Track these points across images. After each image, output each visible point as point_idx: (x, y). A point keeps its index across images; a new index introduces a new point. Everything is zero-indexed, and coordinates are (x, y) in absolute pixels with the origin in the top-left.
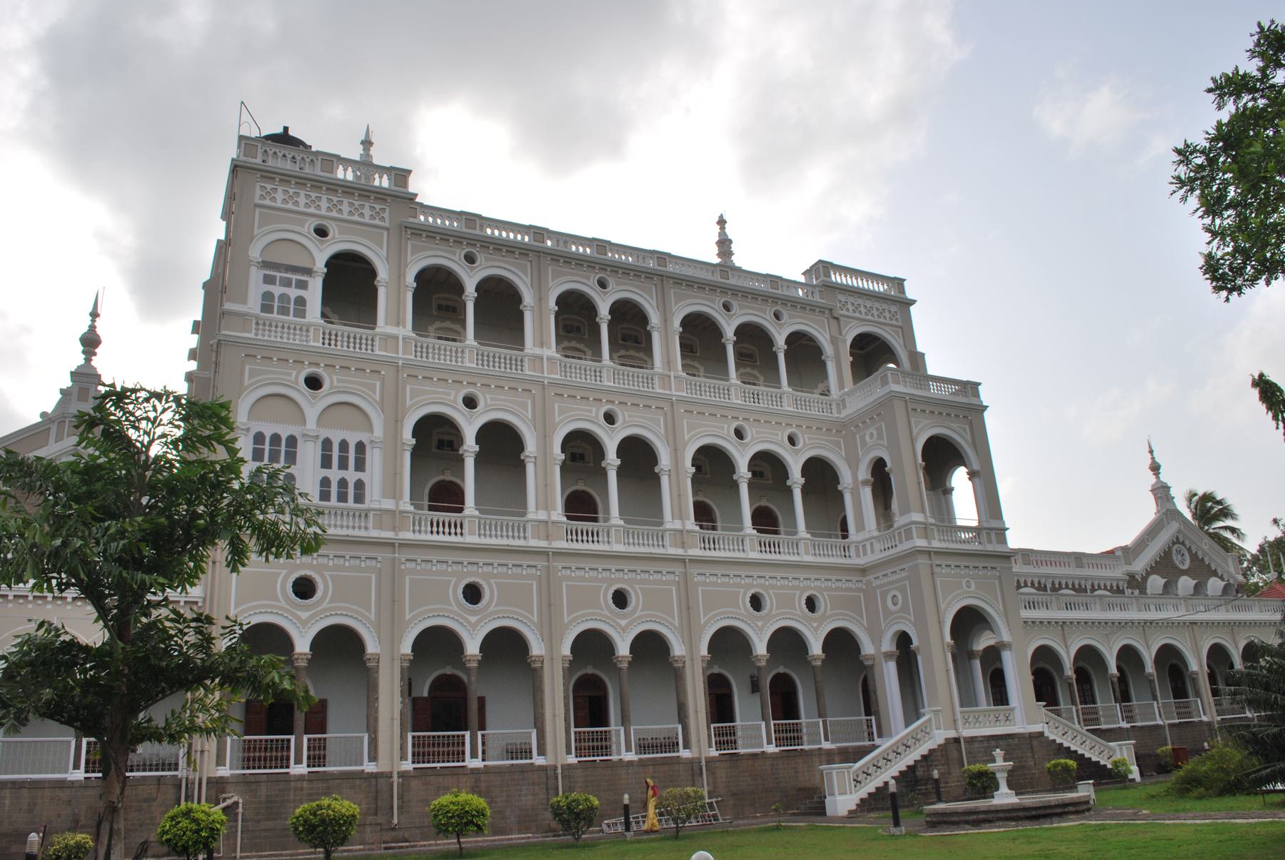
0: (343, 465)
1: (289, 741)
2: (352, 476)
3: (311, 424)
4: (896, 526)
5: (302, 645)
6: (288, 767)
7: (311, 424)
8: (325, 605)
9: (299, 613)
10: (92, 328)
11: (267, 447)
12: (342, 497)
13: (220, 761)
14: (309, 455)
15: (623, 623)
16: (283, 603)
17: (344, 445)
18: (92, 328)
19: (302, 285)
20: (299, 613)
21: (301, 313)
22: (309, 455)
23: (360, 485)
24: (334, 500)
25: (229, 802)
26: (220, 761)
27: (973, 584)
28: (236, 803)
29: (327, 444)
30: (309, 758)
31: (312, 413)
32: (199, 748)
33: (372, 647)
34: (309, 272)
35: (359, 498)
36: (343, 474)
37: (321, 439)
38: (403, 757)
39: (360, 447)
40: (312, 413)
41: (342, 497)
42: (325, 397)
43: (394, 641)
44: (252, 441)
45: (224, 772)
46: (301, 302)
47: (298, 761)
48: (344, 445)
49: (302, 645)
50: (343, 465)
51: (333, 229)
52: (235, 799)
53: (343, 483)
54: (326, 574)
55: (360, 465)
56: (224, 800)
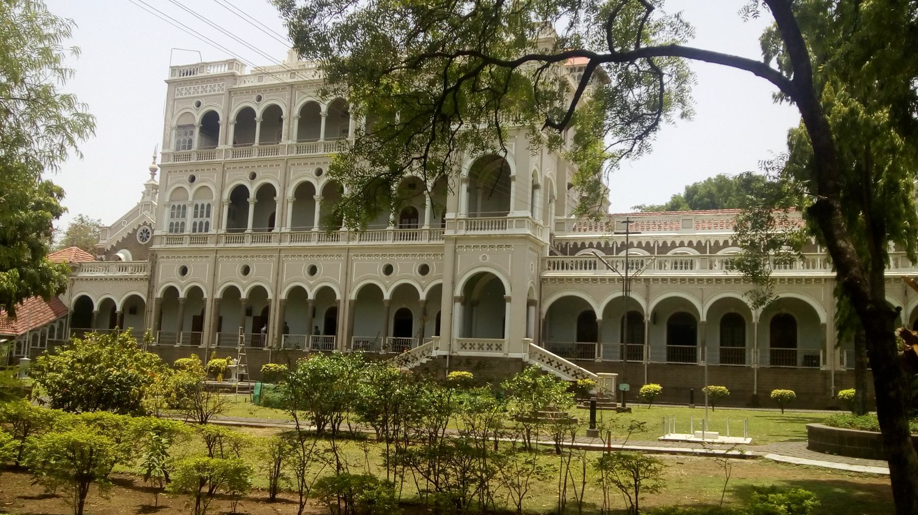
0: (202, 216)
3: (190, 199)
4: (509, 216)
7: (190, 199)
14: (190, 211)
15: (312, 282)
17: (203, 206)
19: (192, 133)
21: (190, 147)
22: (190, 211)
27: (488, 258)
29: (197, 207)
31: (191, 193)
33: (205, 296)
34: (193, 126)
35: (207, 230)
36: (201, 219)
38: (213, 342)
39: (209, 205)
40: (191, 193)
42: (197, 185)
43: (213, 292)
46: (190, 141)
48: (203, 206)
50: (202, 216)
51: (203, 104)
53: (201, 223)
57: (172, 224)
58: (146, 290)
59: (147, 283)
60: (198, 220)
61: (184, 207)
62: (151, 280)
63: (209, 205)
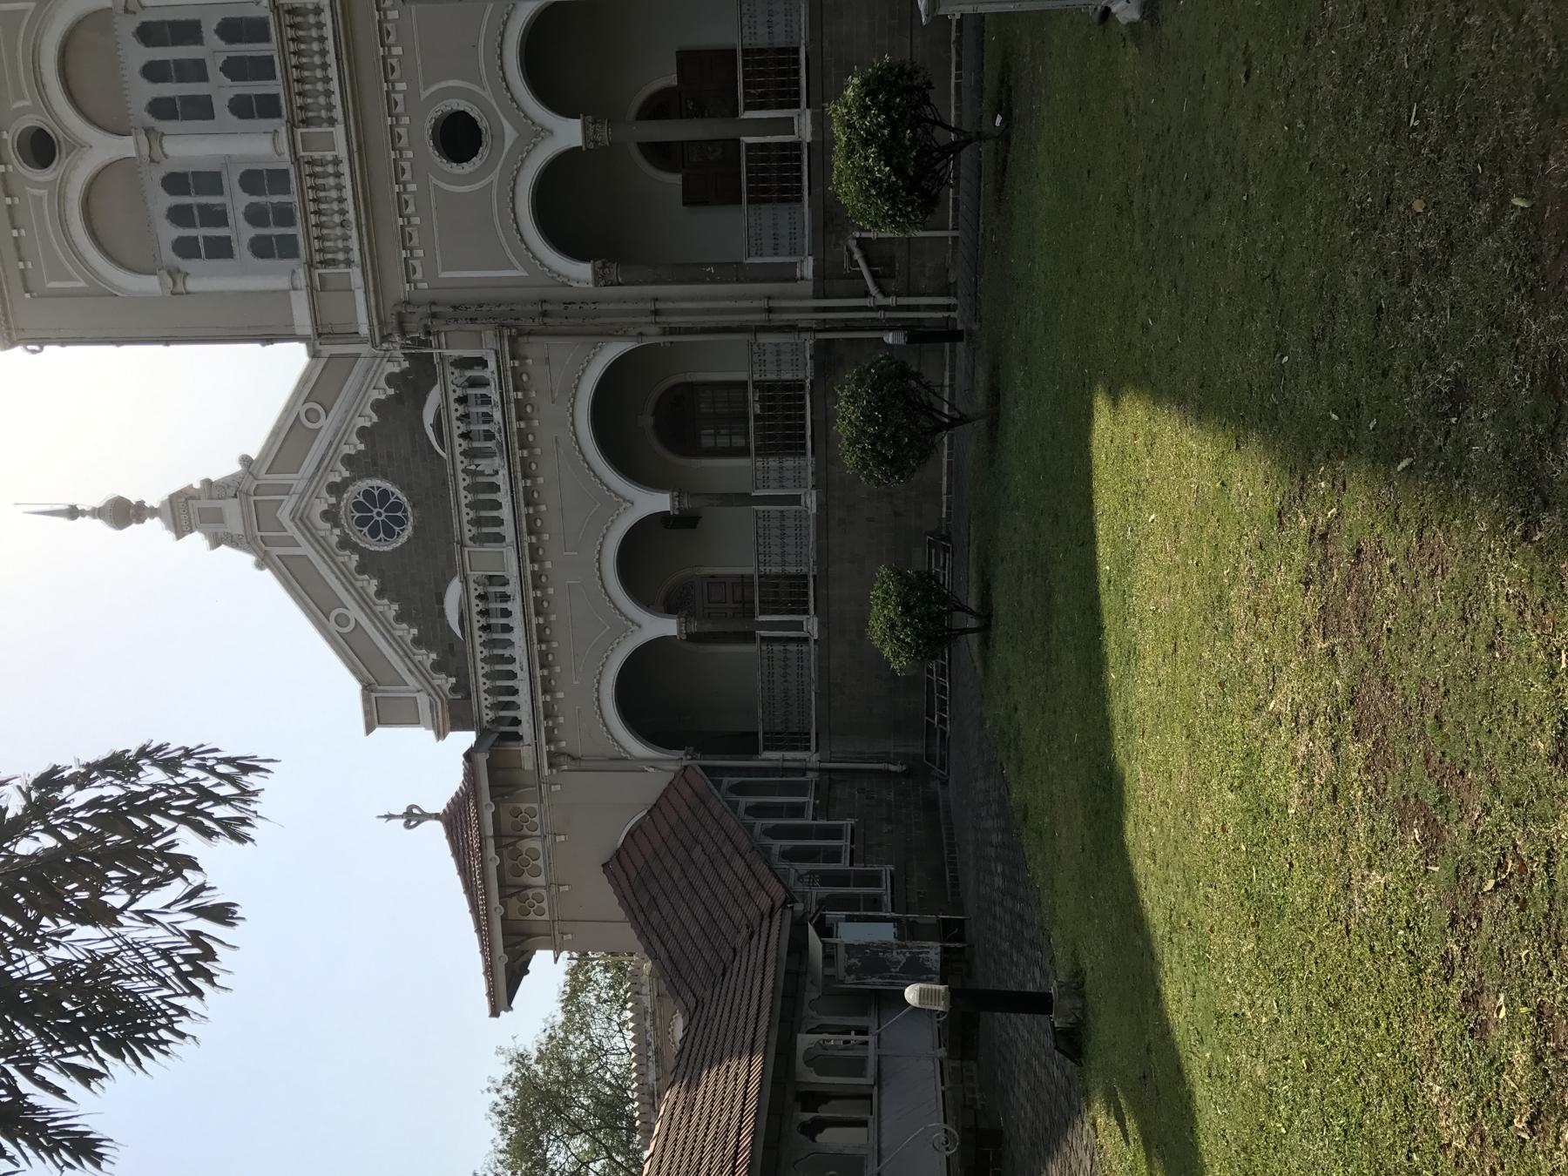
0: (197, 71)
1: (749, 146)
2: (213, 50)
3: (125, 147)
5: (568, 133)
6: (797, 146)
7: (125, 147)
8: (487, 94)
9: (508, 143)
10: (97, 513)
11: (200, 232)
12: (263, 68)
13: (786, 274)
14: (189, 147)
16: (494, 176)
17: (154, 72)
18: (97, 513)
20: (508, 143)
22: (189, 147)
23: (231, 30)
24: (275, 87)
25: (857, 256)
26: (786, 274)
28: (861, 243)
30: (781, 106)
32: (763, 316)
36: (214, 70)
37: (151, 121)
39: (148, 34)
41: (263, 68)
44: (195, 262)
45: (807, 268)
47: (787, 125)
48: (154, 72)
49: (568, 133)
50: (197, 71)
52: (853, 244)
53: (234, 68)
54: (424, 94)
55: (187, 32)
56: (854, 263)
57: (261, 248)
58: (563, 350)
59: (534, 349)
60: (222, 90)
61: (175, 183)
62: (525, 321)
63: (148, 34)
